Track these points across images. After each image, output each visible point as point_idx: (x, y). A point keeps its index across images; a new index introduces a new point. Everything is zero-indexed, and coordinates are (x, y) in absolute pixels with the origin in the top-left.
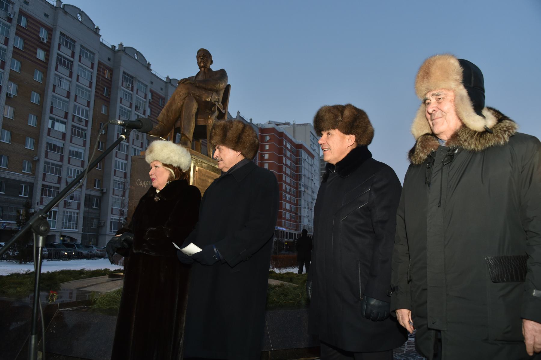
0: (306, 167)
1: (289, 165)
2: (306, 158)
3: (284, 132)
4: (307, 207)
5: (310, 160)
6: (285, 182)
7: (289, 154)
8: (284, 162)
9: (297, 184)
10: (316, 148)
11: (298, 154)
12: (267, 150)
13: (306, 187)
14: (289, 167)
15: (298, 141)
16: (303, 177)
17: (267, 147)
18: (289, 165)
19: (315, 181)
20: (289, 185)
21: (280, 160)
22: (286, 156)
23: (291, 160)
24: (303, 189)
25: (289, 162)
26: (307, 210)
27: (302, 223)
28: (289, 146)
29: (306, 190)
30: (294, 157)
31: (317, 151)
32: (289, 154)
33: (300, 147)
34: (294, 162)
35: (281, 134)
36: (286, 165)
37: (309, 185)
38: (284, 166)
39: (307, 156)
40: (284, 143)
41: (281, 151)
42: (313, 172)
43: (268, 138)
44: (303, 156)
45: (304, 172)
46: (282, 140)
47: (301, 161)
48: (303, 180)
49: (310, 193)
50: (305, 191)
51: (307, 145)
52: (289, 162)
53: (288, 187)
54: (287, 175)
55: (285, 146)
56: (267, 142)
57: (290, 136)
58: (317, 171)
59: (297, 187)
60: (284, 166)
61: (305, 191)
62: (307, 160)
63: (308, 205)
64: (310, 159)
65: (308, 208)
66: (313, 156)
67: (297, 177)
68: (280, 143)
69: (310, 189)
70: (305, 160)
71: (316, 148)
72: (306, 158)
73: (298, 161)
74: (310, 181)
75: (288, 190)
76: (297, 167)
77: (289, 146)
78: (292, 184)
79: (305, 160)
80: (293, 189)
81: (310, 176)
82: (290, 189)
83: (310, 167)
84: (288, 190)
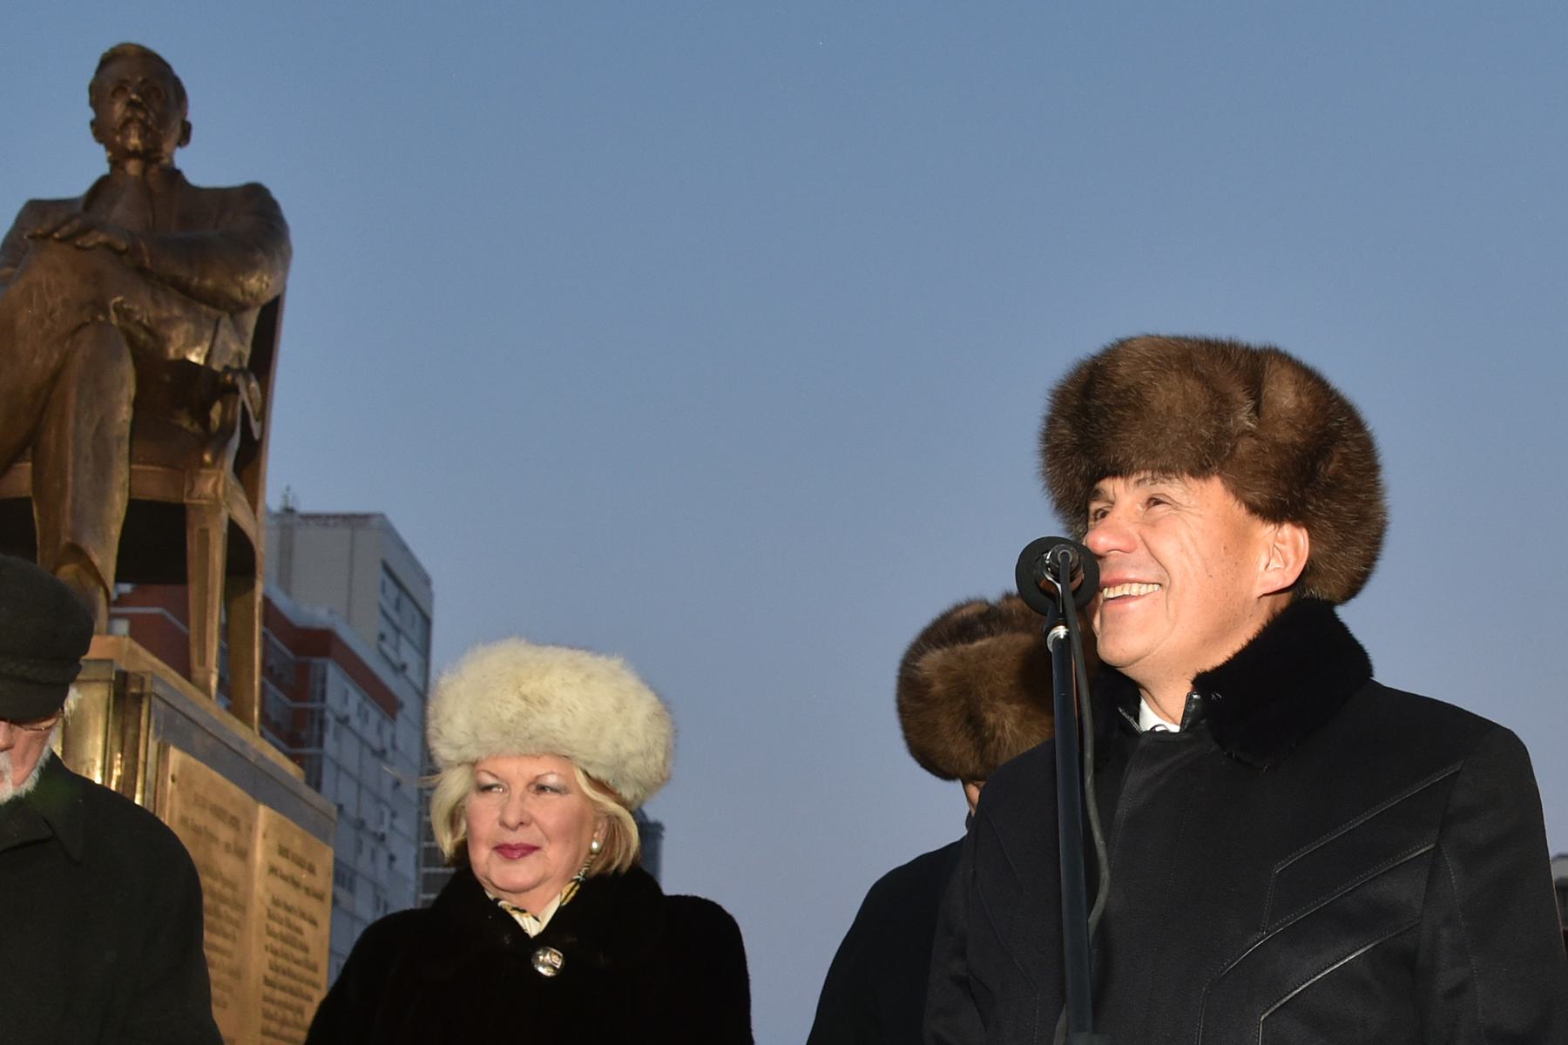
2: (351, 709)
5: (370, 724)
10: (408, 655)
15: (311, 606)
19: (396, 845)
31: (413, 672)
33: (320, 643)
37: (363, 864)
39: (355, 697)
42: (387, 794)
44: (333, 698)
47: (322, 723)
51: (360, 638)
62: (355, 722)
64: (374, 716)
71: (408, 655)
72: (351, 709)
74: (369, 843)
79: (344, 721)
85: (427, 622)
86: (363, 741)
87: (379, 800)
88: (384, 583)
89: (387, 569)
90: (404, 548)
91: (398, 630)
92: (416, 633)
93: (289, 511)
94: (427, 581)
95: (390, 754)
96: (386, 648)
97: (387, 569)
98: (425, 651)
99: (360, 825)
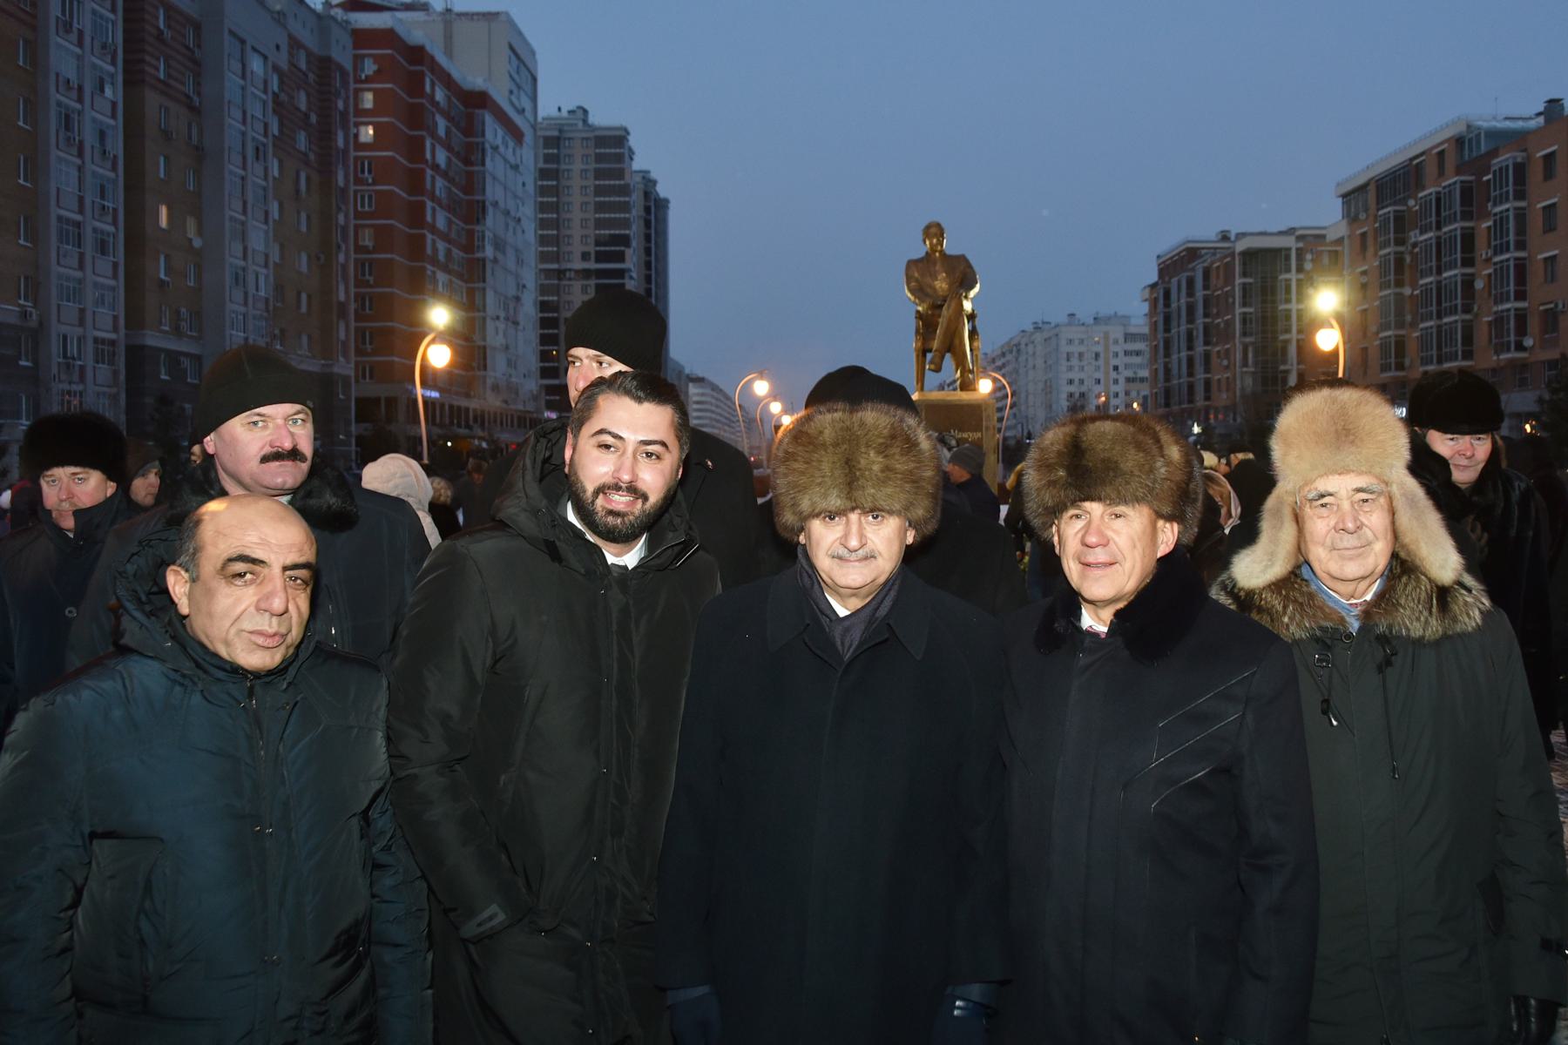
0: (500, 174)
1: (443, 164)
2: (499, 141)
3: (428, 48)
4: (502, 315)
6: (433, 229)
7: (442, 124)
8: (428, 156)
9: (471, 233)
10: (525, 103)
11: (471, 128)
12: (367, 113)
13: (499, 245)
14: (445, 175)
15: (471, 76)
16: (490, 210)
17: (368, 100)
18: (443, 164)
20: (445, 237)
21: (415, 149)
22: (434, 135)
23: (449, 148)
24: (489, 251)
25: (442, 157)
26: (501, 326)
27: (490, 373)
28: (440, 95)
29: (500, 256)
30: (458, 138)
31: (528, 114)
32: (442, 124)
33: (479, 100)
34: (458, 155)
35: (417, 54)
36: (436, 167)
38: (429, 172)
39: (500, 132)
40: (428, 88)
41: (416, 117)
42: (520, 192)
43: (370, 68)
44: (489, 135)
45: (493, 192)
46: (422, 75)
47: (483, 150)
48: (489, 220)
49: (511, 263)
50: (495, 261)
51: (500, 95)
52: (442, 157)
53: (441, 246)
54: (440, 205)
55: (432, 98)
56: (368, 80)
57: (442, 59)
58: (530, 188)
59: (470, 244)
60: (429, 172)
61: (495, 261)
62: (502, 149)
63: (506, 309)
64: (511, 144)
65: (507, 319)
66: (516, 134)
67: (471, 209)
68: (414, 85)
69: (510, 253)
70: (495, 148)
71: (525, 103)
72: (499, 141)
73: (471, 153)
74: (512, 224)
75: (441, 257)
76: (470, 175)
77: (440, 95)
78: (453, 235)
79: (495, 148)
80: (455, 251)
81: (511, 205)
82: (448, 253)
83: (510, 173)
84: (441, 257)
85: (535, 79)
86: (506, 161)
87: (516, 196)
88: (449, 52)
89: (512, 48)
90: (520, 34)
91: (519, 87)
92: (528, 88)
93: (449, 11)
94: (533, 53)
95: (521, 168)
96: (513, 98)
97: (512, 48)
98: (534, 99)
99: (507, 213)
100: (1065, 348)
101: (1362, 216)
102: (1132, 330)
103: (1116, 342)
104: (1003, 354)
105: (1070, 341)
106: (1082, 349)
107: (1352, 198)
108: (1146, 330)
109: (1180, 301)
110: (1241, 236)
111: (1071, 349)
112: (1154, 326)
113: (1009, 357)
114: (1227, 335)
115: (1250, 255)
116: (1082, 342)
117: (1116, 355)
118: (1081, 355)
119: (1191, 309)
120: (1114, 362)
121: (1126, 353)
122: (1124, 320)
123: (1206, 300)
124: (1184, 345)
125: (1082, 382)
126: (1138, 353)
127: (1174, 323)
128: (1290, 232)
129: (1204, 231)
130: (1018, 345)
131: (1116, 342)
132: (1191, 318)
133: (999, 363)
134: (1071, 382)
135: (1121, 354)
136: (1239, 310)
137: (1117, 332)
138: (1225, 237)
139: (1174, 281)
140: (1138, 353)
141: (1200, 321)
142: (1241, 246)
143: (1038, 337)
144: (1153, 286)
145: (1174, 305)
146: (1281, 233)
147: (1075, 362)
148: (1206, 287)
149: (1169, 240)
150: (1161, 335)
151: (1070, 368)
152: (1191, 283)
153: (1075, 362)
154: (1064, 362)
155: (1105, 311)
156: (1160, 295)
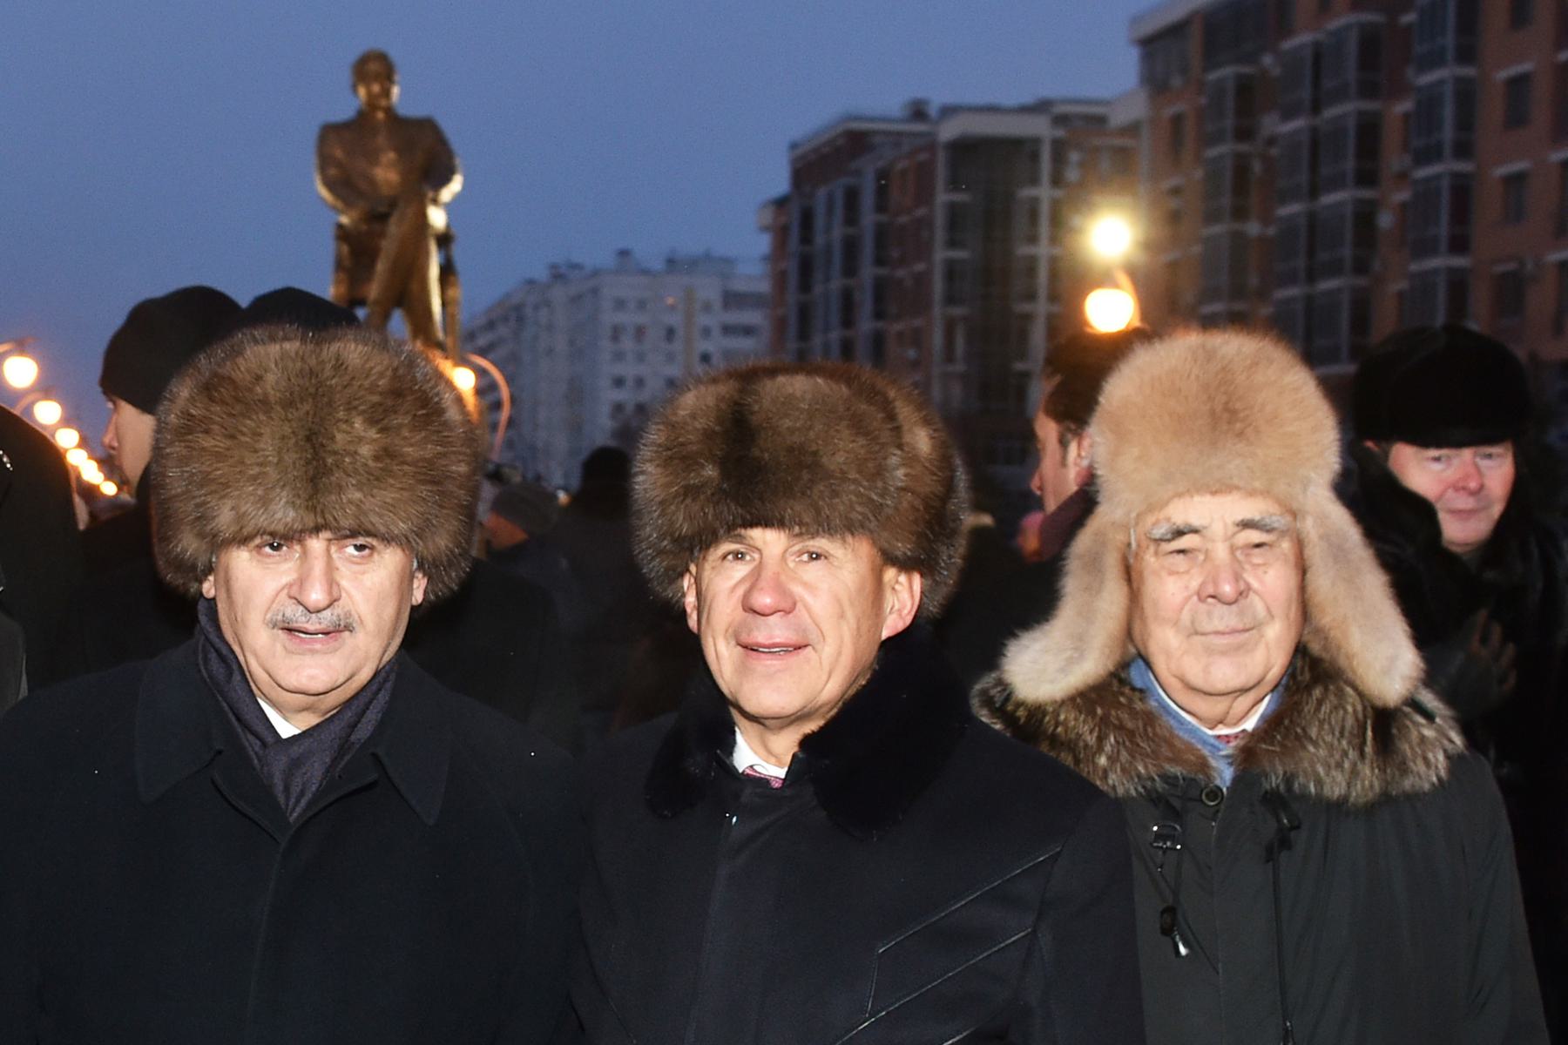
100: (609, 318)
101: (1176, 82)
102: (740, 286)
103: (707, 308)
104: (491, 325)
105: (620, 304)
106: (641, 319)
107: (1157, 45)
108: (764, 287)
109: (830, 233)
110: (949, 111)
111: (622, 318)
112: (780, 280)
113: (503, 330)
114: (917, 300)
115: (967, 151)
116: (642, 305)
117: (706, 332)
118: (640, 332)
119: (851, 248)
120: (703, 346)
121: (728, 330)
122: (722, 265)
123: (881, 234)
124: (835, 318)
125: (640, 382)
126: (748, 331)
127: (818, 276)
128: (1040, 107)
129: (879, 98)
130: (518, 308)
131: (707, 308)
132: (850, 269)
133: (482, 341)
134: (619, 382)
135: (716, 332)
136: (940, 254)
137: (708, 289)
138: (918, 112)
139: (822, 193)
140: (748, 331)
141: (868, 271)
142: (949, 131)
143: (559, 294)
144: (781, 203)
145: (819, 240)
146: (1024, 110)
147: (627, 344)
148: (881, 207)
149: (814, 114)
150: (792, 297)
151: (619, 356)
152: (852, 197)
153: (627, 344)
154: (606, 344)
155: (690, 246)
156: (794, 220)
